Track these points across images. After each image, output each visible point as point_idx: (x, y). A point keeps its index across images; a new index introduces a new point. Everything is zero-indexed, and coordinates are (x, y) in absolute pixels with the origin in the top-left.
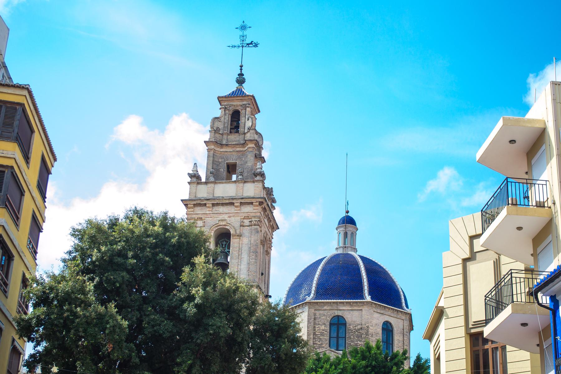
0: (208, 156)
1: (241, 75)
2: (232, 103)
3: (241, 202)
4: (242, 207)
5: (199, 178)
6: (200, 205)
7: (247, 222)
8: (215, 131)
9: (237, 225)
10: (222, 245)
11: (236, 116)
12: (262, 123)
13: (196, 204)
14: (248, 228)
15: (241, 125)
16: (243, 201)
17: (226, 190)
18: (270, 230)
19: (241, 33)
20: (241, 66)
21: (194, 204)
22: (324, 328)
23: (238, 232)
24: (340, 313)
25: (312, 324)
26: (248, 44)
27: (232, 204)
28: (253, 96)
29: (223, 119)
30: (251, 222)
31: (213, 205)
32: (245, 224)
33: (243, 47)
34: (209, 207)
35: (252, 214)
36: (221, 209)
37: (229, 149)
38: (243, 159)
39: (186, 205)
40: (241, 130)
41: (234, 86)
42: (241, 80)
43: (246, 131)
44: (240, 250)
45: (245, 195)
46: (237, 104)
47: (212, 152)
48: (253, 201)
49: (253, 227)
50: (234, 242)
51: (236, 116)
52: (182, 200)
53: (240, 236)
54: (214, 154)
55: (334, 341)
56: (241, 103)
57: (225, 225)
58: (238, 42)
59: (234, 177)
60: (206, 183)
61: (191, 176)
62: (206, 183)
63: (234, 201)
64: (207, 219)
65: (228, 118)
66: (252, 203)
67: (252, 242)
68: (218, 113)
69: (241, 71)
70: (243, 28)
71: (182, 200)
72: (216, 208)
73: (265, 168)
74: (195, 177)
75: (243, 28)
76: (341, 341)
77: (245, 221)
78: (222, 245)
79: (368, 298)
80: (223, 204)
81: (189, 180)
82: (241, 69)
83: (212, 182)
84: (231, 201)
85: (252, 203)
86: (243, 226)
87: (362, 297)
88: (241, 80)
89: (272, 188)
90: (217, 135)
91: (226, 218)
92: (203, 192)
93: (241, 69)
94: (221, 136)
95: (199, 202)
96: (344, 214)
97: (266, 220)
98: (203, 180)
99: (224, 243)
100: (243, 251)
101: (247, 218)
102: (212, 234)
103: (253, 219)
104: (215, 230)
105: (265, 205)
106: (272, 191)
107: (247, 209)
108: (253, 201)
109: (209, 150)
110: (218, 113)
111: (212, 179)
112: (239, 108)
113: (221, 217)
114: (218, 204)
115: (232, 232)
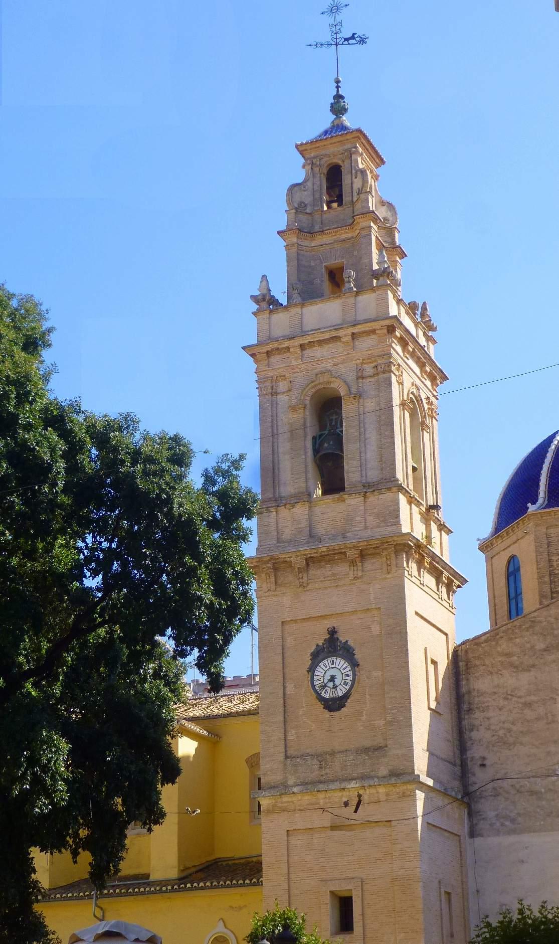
0: (289, 260)
1: (338, 97)
2: (323, 152)
3: (353, 334)
4: (357, 343)
5: (273, 301)
7: (369, 369)
8: (297, 209)
9: (351, 377)
13: (272, 350)
16: (356, 330)
18: (428, 383)
19: (332, 21)
21: (268, 353)
23: (354, 390)
25: (545, 555)
26: (346, 39)
27: (336, 339)
28: (359, 131)
29: (309, 184)
33: (336, 44)
35: (376, 352)
36: (318, 352)
38: (355, 253)
39: (253, 355)
40: (346, 198)
41: (328, 119)
42: (338, 107)
44: (361, 424)
46: (333, 152)
47: (295, 250)
49: (381, 376)
50: (348, 408)
52: (244, 348)
53: (359, 396)
54: (298, 254)
56: (341, 149)
58: (327, 37)
61: (253, 297)
63: (341, 333)
64: (296, 375)
66: (373, 331)
69: (338, 91)
71: (244, 348)
72: (308, 352)
74: (266, 302)
77: (366, 366)
80: (321, 343)
81: (255, 307)
82: (338, 87)
83: (296, 305)
84: (334, 334)
85: (373, 331)
86: (363, 378)
88: (338, 107)
89: (424, 304)
90: (302, 217)
91: (330, 368)
93: (338, 87)
94: (310, 218)
95: (275, 345)
97: (411, 363)
100: (367, 426)
101: (370, 359)
102: (308, 402)
104: (310, 393)
106: (426, 309)
109: (287, 247)
110: (299, 175)
111: (297, 299)
114: (311, 344)
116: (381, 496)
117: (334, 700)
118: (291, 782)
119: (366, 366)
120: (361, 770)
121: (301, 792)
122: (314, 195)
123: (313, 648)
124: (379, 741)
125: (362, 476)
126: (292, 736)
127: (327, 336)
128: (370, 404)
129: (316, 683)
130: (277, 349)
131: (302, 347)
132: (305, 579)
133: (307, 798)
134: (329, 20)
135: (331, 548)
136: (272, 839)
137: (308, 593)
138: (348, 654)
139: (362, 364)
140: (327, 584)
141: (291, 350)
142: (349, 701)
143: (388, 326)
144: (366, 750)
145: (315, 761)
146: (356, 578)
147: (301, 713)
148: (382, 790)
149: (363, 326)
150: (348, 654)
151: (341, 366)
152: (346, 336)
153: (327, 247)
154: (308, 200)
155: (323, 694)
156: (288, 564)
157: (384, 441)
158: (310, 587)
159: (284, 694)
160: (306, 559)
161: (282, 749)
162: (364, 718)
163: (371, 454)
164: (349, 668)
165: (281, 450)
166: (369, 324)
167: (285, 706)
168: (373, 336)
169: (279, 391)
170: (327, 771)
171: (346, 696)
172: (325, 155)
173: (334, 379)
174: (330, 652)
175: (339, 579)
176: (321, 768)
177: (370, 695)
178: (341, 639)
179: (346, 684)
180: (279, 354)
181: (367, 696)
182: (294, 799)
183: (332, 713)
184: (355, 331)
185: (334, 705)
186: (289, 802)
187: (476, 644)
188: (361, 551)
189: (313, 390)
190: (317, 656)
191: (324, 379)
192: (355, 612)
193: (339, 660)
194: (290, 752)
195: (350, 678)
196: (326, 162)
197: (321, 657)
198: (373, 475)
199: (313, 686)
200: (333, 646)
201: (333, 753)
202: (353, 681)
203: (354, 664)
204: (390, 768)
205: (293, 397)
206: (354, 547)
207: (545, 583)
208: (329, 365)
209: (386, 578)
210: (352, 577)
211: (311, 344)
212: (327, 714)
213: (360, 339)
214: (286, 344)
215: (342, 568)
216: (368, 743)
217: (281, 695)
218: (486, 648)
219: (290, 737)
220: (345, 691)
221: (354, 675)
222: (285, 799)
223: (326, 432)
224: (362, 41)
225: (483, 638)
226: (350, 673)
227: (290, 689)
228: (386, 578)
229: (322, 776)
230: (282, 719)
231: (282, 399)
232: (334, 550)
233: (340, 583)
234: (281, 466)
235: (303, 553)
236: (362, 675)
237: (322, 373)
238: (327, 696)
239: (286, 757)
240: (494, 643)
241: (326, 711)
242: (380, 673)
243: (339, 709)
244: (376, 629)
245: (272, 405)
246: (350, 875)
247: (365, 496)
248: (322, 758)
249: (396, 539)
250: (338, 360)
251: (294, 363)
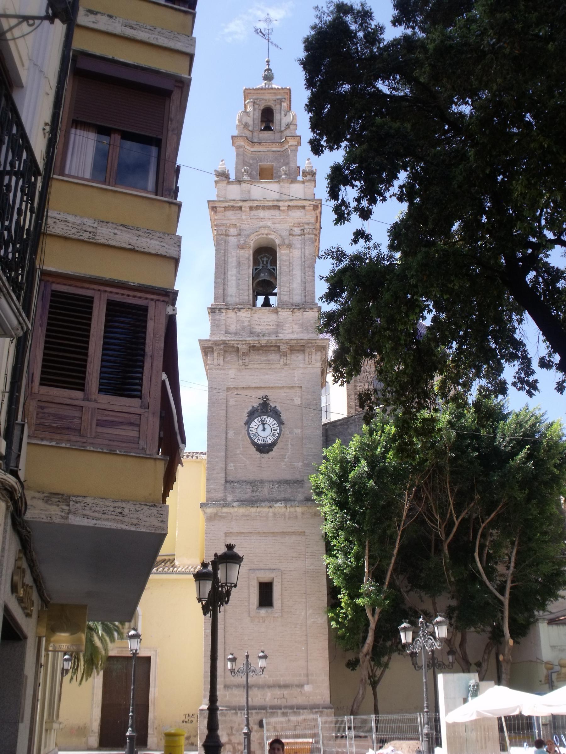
2: (262, 97)
3: (289, 206)
4: (290, 212)
6: (233, 208)
7: (297, 231)
9: (285, 233)
10: (263, 261)
13: (229, 206)
14: (299, 237)
16: (291, 203)
20: (268, 62)
21: (225, 207)
27: (278, 207)
28: (290, 90)
30: (303, 230)
31: (251, 208)
32: (294, 233)
34: (245, 211)
36: (261, 213)
42: (268, 77)
43: (283, 129)
44: (290, 264)
48: (306, 203)
50: (282, 255)
56: (274, 98)
57: (268, 234)
63: (280, 204)
64: (244, 225)
67: (307, 255)
71: (209, 202)
72: (254, 213)
77: (294, 228)
78: (263, 261)
80: (264, 208)
84: (276, 203)
85: (304, 207)
88: (268, 77)
91: (270, 225)
92: (234, 192)
93: (268, 65)
95: (232, 204)
99: (265, 259)
100: (294, 267)
101: (299, 225)
103: (306, 227)
107: (298, 214)
108: (306, 203)
112: (271, 104)
113: (262, 224)
114: (257, 208)
115: (278, 242)
116: (305, 313)
117: (264, 446)
118: (229, 499)
119: (294, 228)
120: (283, 495)
121: (239, 506)
122: (254, 121)
123: (250, 408)
124: (298, 477)
125: (290, 299)
126: (231, 466)
127: (271, 204)
128: (296, 253)
129: (251, 432)
130: (232, 206)
131: (251, 208)
132: (247, 361)
133: (242, 510)
135: (269, 341)
136: (213, 538)
137: (248, 371)
138: (276, 414)
139: (293, 226)
140: (263, 366)
141: (243, 209)
142: (275, 447)
143: (314, 205)
144: (287, 482)
145: (249, 486)
146: (286, 364)
147: (238, 452)
148: (299, 510)
149: (297, 202)
150: (276, 414)
151: (278, 225)
152: (284, 206)
153: (262, 153)
155: (256, 441)
156: (237, 350)
157: (307, 278)
158: (250, 366)
159: (226, 438)
160: (249, 347)
161: (223, 475)
162: (286, 460)
163: (296, 285)
164: (277, 425)
165: (229, 273)
166: (300, 202)
167: (226, 446)
168: (302, 210)
169: (230, 234)
170: (258, 494)
171: (274, 444)
172: (263, 99)
173: (273, 233)
174: (263, 412)
175: (272, 364)
176: (253, 491)
177: (292, 445)
178: (271, 404)
179: (274, 435)
180: (233, 210)
181: (290, 446)
182: (231, 510)
183: (262, 455)
184: (290, 204)
185: (264, 449)
186: (227, 513)
187: (334, 426)
188: (291, 346)
189: (257, 238)
190: (252, 415)
191: (266, 231)
192: (281, 388)
193: (269, 418)
194: (230, 478)
195: (278, 432)
197: (256, 415)
198: (297, 298)
199: (249, 435)
200: (264, 409)
201: (262, 482)
202: (280, 434)
203: (281, 423)
204: (306, 495)
205: (242, 239)
206: (287, 343)
207: (351, 399)
208: (269, 223)
209: (307, 368)
210: (282, 363)
211: (257, 208)
212: (258, 455)
213: (293, 211)
214: (240, 204)
215: (274, 357)
216: (288, 477)
217: (224, 438)
218: (341, 429)
219: (229, 468)
220: (272, 440)
221: (281, 430)
222: (225, 510)
223: (261, 267)
225: (339, 423)
226: (278, 428)
227: (231, 435)
228: (307, 368)
229: (254, 497)
230: (223, 454)
231: (233, 240)
232: (271, 343)
233: (273, 367)
234: (229, 283)
235: (248, 342)
236: (286, 430)
237: (264, 227)
238: (259, 442)
239: (226, 482)
240: (346, 427)
241: (258, 453)
242: (299, 431)
243: (268, 452)
244: (297, 401)
245: (225, 242)
246: (273, 567)
247: (293, 311)
248: (254, 484)
249: (318, 341)
250: (276, 221)
251: (244, 217)
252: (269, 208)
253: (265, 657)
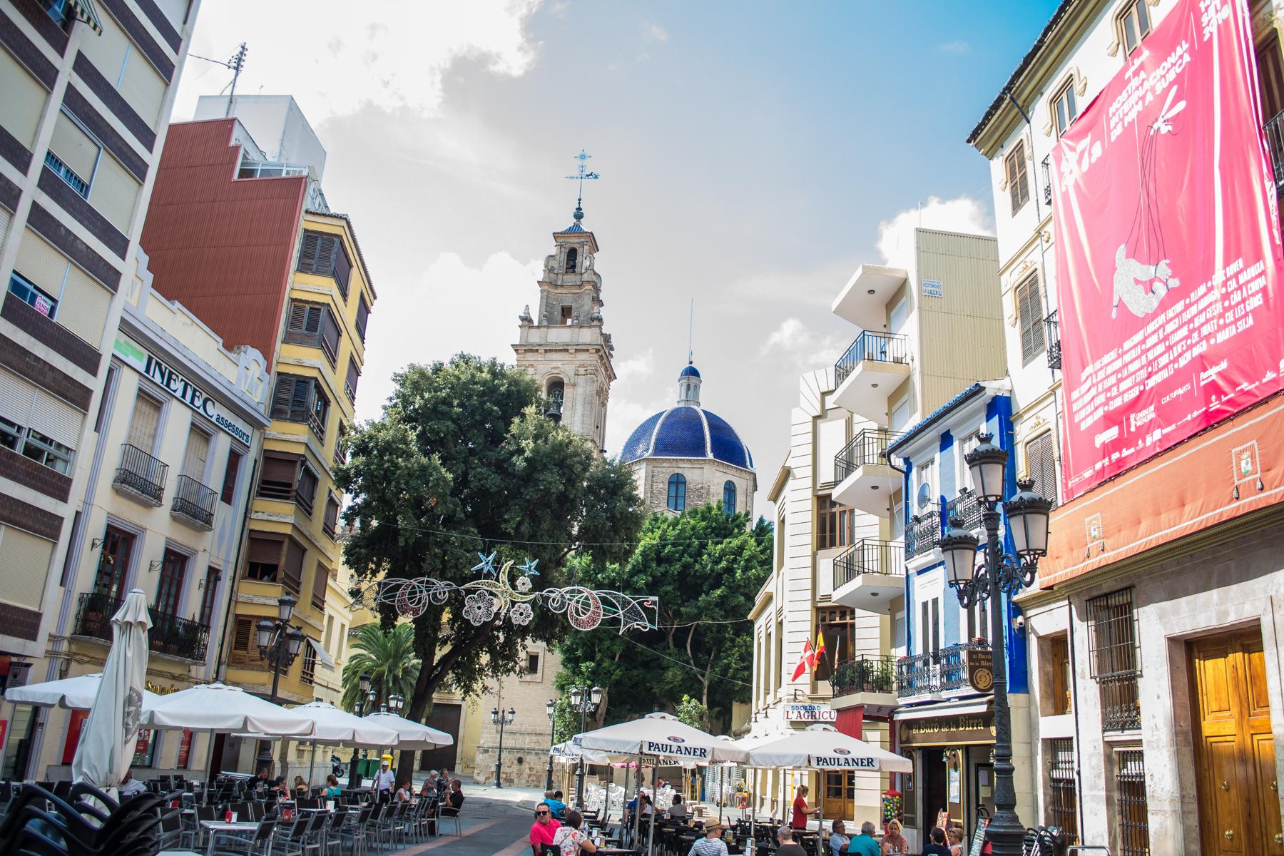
1: (579, 209)
5: (530, 321)
6: (532, 351)
7: (582, 371)
8: (549, 270)
11: (572, 254)
12: (602, 263)
15: (578, 264)
17: (559, 335)
22: (662, 486)
24: (680, 471)
31: (546, 351)
36: (554, 356)
37: (563, 291)
40: (577, 270)
42: (579, 215)
44: (574, 400)
45: (581, 341)
46: (574, 241)
51: (572, 254)
55: (672, 501)
58: (577, 174)
59: (569, 322)
60: (538, 327)
61: (522, 319)
62: (538, 327)
65: (564, 257)
68: (553, 250)
70: (583, 157)
73: (603, 312)
74: (526, 320)
75: (583, 157)
76: (680, 501)
79: (710, 456)
80: (556, 351)
87: (704, 454)
88: (579, 215)
92: (535, 337)
96: (688, 365)
98: (536, 323)
101: (583, 366)
105: (602, 353)
107: (583, 357)
109: (542, 291)
110: (553, 250)
111: (545, 323)
112: (577, 246)
113: (554, 364)
114: (551, 351)
134: (579, 162)
154: (556, 266)
196: (569, 246)
224: (596, 177)
252: (561, 351)
253: (513, 713)
